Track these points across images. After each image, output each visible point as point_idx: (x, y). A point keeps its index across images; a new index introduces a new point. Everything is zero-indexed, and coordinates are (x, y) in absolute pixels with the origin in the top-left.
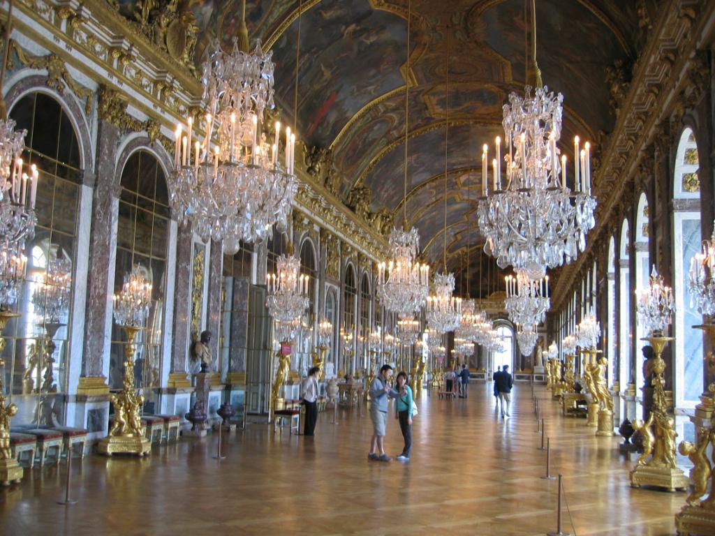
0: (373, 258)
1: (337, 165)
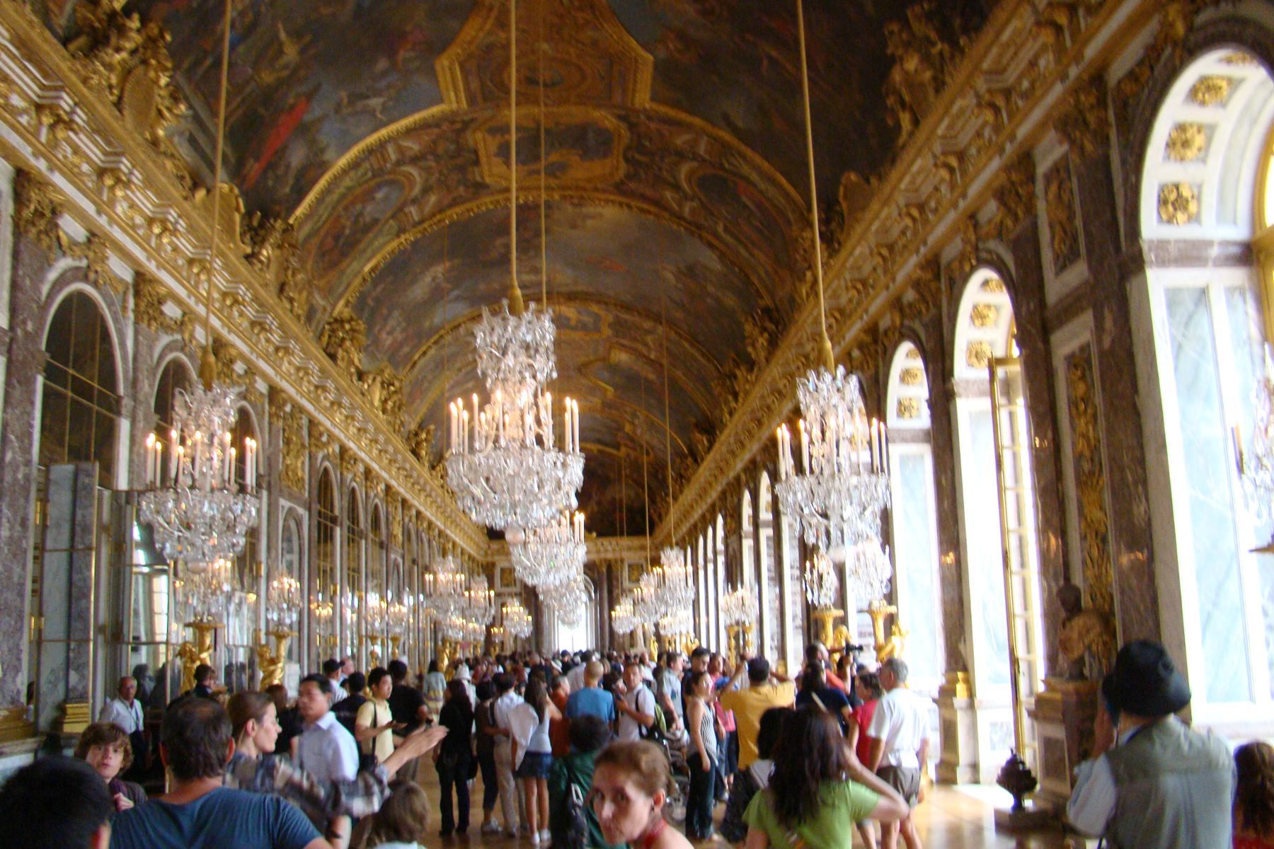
1: (302, 261)
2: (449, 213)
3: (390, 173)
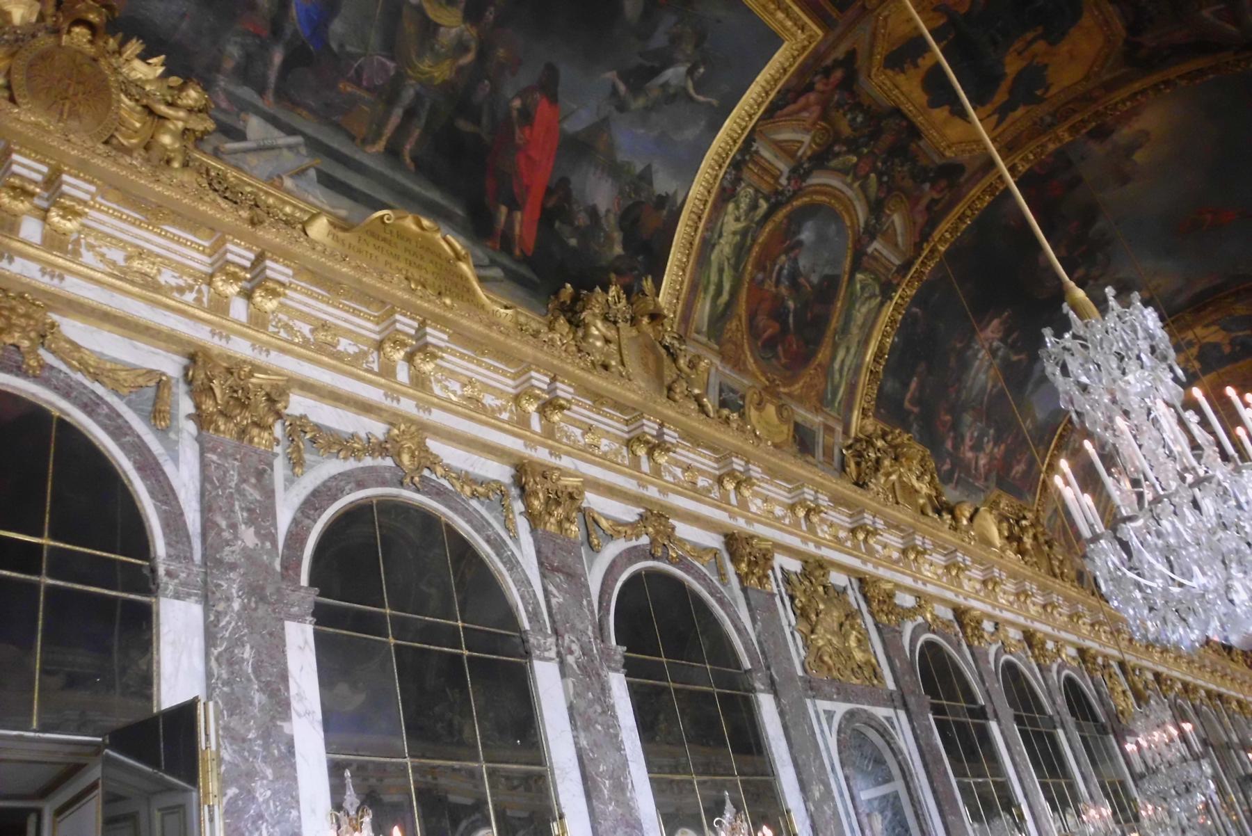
0: (1021, 620)
2: (936, 235)
3: (796, 194)
